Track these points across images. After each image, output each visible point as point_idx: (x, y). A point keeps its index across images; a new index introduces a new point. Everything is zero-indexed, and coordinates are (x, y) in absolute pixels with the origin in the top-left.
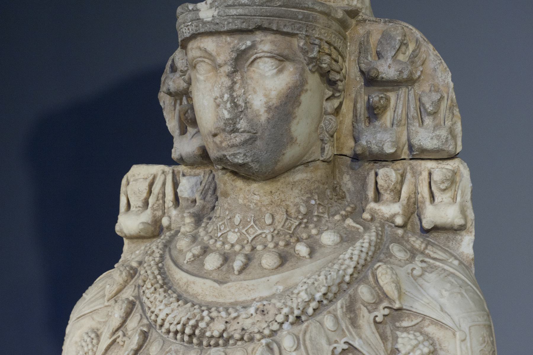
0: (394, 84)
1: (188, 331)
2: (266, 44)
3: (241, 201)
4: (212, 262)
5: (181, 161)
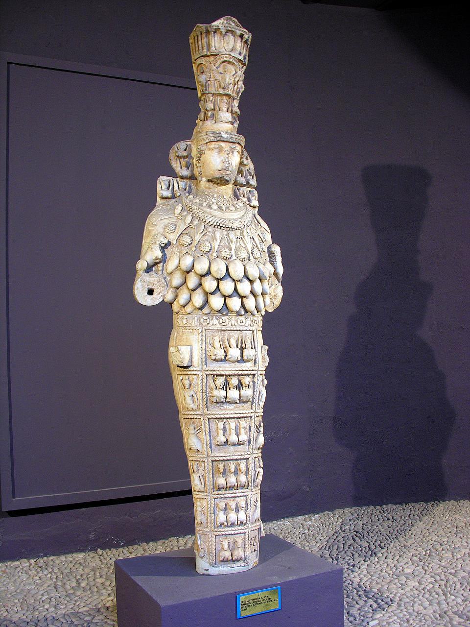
0: (245, 165)
1: (221, 225)
2: (238, 148)
3: (216, 191)
4: (215, 207)
5: (182, 177)
